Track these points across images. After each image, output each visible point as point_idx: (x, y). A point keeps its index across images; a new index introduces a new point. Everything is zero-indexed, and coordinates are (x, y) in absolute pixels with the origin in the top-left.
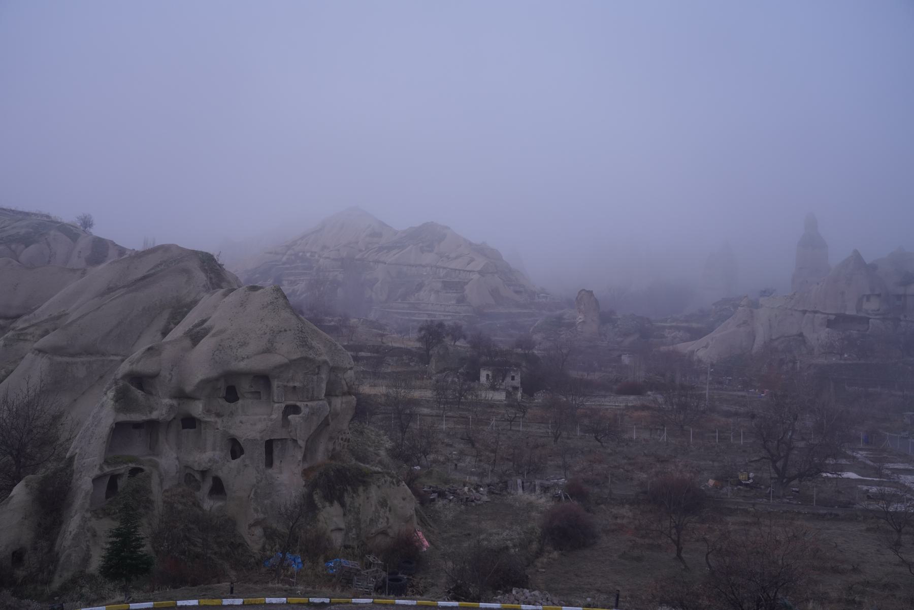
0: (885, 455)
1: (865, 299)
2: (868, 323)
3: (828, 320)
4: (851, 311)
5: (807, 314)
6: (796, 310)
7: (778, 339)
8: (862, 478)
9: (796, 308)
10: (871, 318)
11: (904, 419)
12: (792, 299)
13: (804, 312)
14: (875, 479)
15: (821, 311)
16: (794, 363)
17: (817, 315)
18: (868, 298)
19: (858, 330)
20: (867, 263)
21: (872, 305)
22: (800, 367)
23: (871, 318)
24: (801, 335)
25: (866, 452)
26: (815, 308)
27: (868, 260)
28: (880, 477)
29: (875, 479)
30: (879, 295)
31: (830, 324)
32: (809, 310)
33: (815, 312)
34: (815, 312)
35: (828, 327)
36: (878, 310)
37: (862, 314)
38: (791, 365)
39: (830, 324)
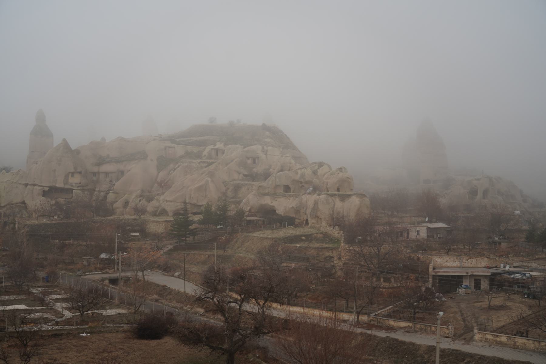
0: (55, 290)
1: (70, 176)
2: (72, 192)
3: (44, 191)
4: (60, 184)
5: (28, 187)
6: (20, 184)
7: (5, 206)
8: (27, 308)
9: (20, 182)
10: (74, 189)
11: (83, 261)
12: (18, 175)
13: (26, 185)
14: (37, 308)
15: (38, 184)
16: (15, 224)
17: (35, 187)
18: (73, 174)
19: (66, 198)
20: (73, 148)
21: (75, 180)
22: (18, 227)
23: (74, 189)
24: (24, 202)
25: (43, 289)
26: (34, 181)
27: (73, 147)
28: (43, 306)
29: (37, 308)
30: (80, 173)
31: (45, 194)
32: (30, 183)
33: (34, 185)
34: (34, 185)
35: (43, 196)
36: (80, 183)
37: (67, 186)
38: (12, 225)
39: (45, 194)
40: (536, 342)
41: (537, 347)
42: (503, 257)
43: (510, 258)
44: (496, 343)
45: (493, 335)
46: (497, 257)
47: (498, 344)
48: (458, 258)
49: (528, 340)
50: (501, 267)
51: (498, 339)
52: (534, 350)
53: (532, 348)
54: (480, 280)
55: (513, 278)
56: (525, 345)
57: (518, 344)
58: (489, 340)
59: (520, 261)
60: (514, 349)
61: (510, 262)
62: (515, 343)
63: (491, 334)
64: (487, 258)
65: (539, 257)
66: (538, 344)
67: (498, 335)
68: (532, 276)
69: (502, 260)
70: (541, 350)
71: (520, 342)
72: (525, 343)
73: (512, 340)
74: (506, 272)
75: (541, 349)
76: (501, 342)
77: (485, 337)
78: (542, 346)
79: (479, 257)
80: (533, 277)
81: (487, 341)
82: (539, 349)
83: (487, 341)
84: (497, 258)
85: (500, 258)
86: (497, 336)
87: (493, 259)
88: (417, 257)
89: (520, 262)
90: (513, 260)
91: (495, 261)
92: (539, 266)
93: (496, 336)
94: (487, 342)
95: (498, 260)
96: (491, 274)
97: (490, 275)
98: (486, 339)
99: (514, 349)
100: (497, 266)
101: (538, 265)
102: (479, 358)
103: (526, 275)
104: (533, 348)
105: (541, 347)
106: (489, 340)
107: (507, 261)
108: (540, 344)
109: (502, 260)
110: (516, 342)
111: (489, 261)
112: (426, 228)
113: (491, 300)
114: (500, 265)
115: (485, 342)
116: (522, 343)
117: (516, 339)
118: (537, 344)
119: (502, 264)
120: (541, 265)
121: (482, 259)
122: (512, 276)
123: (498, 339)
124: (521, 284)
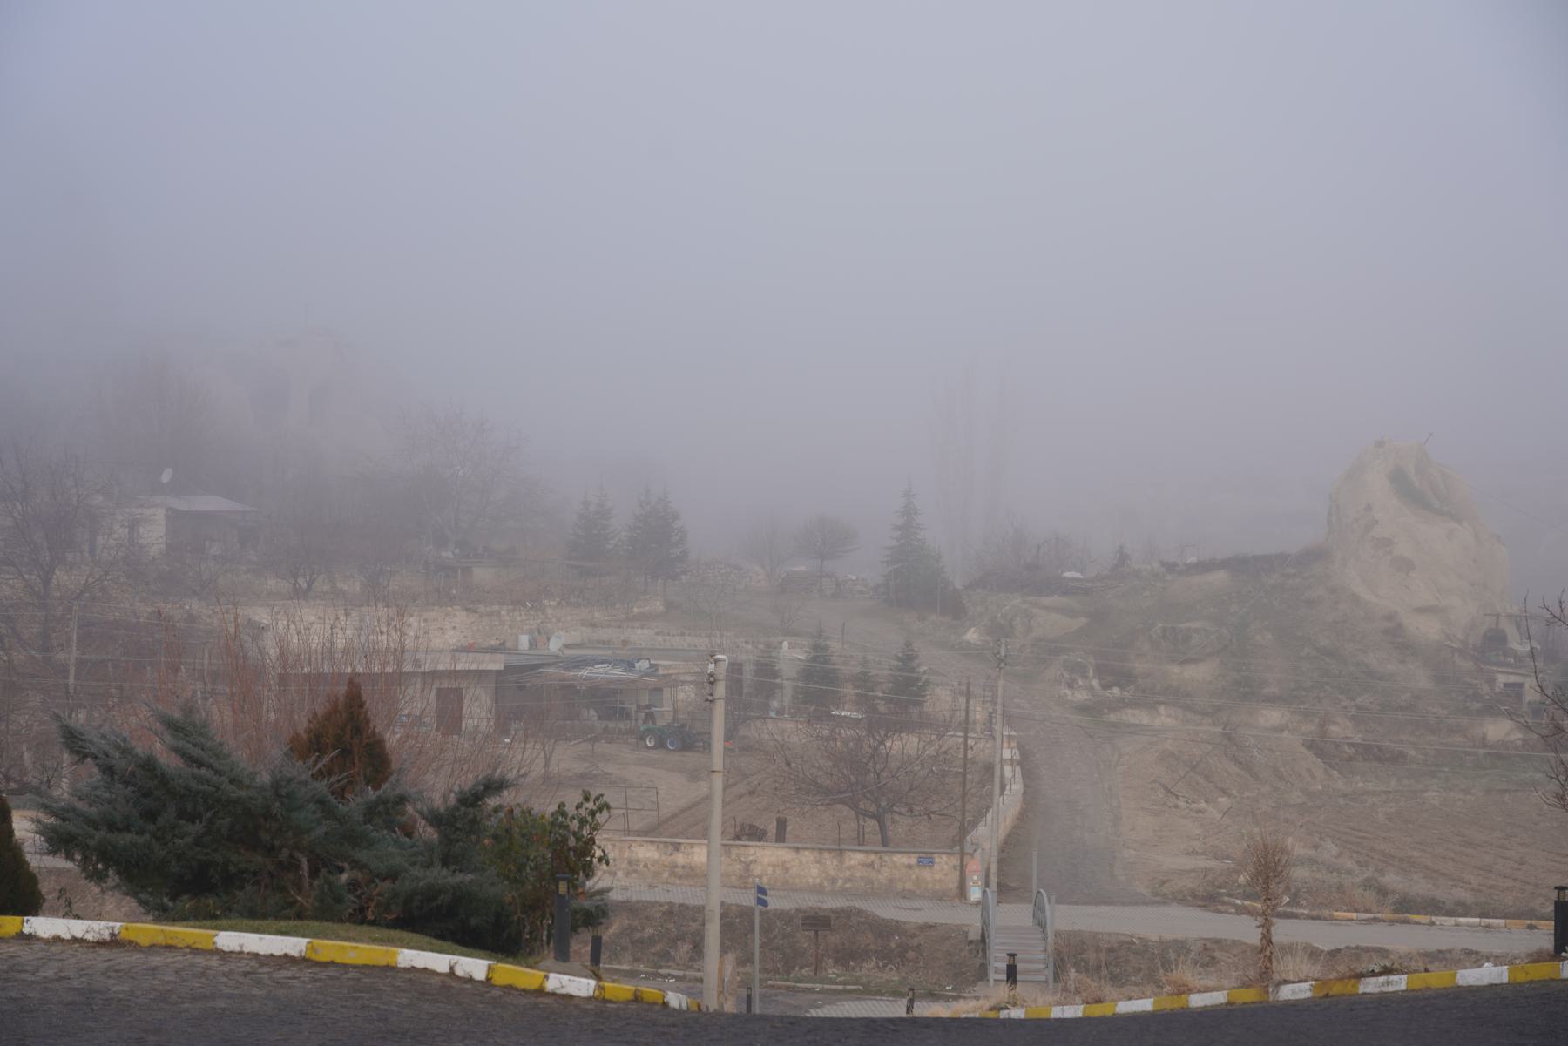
40: (826, 855)
41: (832, 873)
42: (525, 606)
43: (549, 611)
44: (672, 874)
45: (661, 846)
46: (505, 608)
47: (680, 878)
48: (354, 614)
49: (797, 849)
50: (520, 647)
51: (680, 859)
52: (821, 885)
53: (811, 880)
54: (458, 692)
55: (588, 679)
56: (787, 870)
57: (757, 870)
58: (645, 866)
59: (583, 625)
60: (744, 891)
61: (549, 625)
62: (747, 866)
63: (652, 842)
64: (467, 610)
65: (642, 610)
66: (835, 862)
67: (679, 844)
68: (657, 670)
69: (523, 617)
70: (848, 885)
71: (766, 860)
72: (784, 863)
73: (734, 857)
74: (555, 660)
75: (849, 880)
76: (692, 869)
77: (627, 855)
78: (849, 868)
79: (436, 608)
80: (661, 672)
81: (636, 871)
82: (840, 882)
83: (636, 871)
84: (503, 613)
85: (514, 610)
86: (677, 847)
87: (490, 614)
88: (188, 611)
89: (584, 629)
90: (559, 620)
91: (497, 623)
92: (660, 638)
93: (671, 848)
94: (634, 875)
95: (508, 618)
96: (505, 667)
97: (498, 672)
98: (630, 863)
99: (745, 888)
100: (503, 644)
101: (657, 634)
102: (664, 913)
103: (637, 665)
104: (818, 881)
105: (848, 873)
106: (645, 866)
107: (539, 621)
108: (841, 862)
109: (523, 617)
110: (751, 862)
111: (472, 623)
112: (160, 513)
113: (551, 756)
114: (517, 640)
115: (628, 874)
116: (774, 866)
117: (752, 851)
118: (830, 861)
119: (522, 633)
120: (669, 635)
121: (447, 614)
122: (585, 673)
123: (680, 859)
124: (607, 700)
